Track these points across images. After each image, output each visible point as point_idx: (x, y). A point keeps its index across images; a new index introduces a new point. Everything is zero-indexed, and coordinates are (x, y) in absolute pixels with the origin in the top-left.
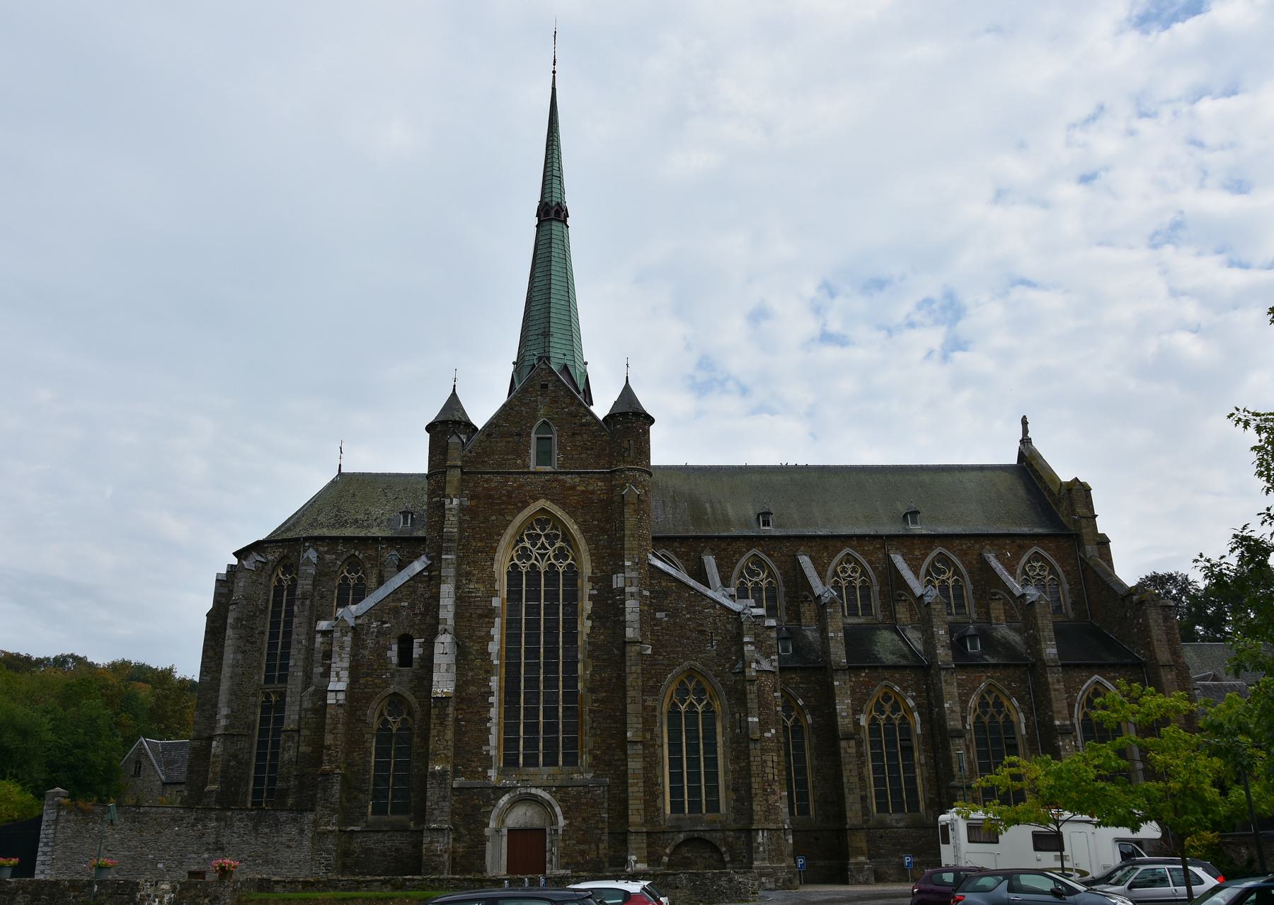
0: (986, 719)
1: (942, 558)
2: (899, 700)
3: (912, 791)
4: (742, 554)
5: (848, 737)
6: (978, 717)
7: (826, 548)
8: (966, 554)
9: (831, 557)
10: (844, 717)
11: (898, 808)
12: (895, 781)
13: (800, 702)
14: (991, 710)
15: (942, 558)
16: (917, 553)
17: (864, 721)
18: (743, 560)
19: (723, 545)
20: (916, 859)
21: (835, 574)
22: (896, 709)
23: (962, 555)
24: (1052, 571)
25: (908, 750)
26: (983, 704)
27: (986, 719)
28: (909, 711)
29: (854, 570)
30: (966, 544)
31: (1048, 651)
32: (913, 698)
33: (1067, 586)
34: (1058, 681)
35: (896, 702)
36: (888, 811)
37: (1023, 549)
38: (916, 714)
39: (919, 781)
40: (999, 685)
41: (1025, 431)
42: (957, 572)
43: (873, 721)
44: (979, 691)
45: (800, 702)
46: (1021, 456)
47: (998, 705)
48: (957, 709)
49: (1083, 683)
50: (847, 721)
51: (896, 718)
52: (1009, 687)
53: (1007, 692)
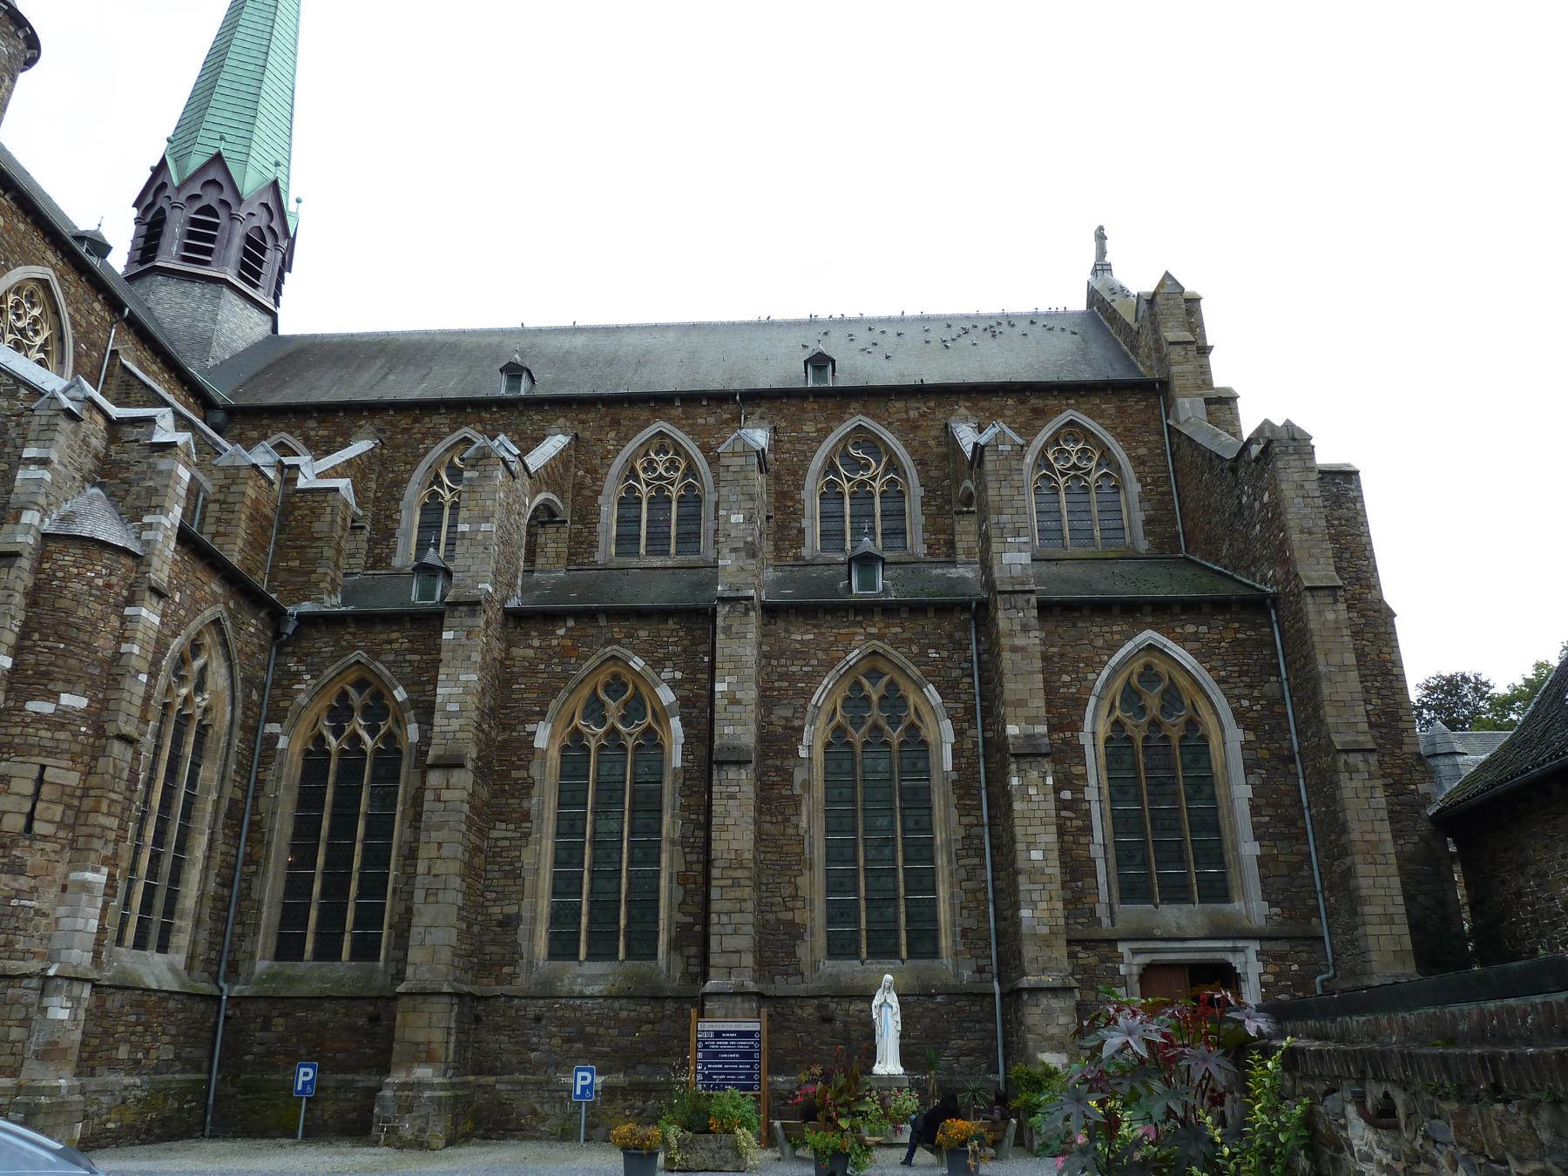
0: (858, 737)
1: (863, 438)
2: (644, 690)
3: (645, 906)
4: (438, 438)
5: (451, 764)
6: (839, 731)
7: (616, 423)
8: (915, 428)
9: (624, 439)
10: (449, 716)
11: (602, 948)
12: (605, 875)
13: (400, 694)
14: (875, 715)
15: (863, 438)
16: (809, 428)
17: (543, 736)
18: (440, 448)
19: (404, 422)
20: (620, 1079)
21: (633, 474)
22: (634, 710)
23: (908, 429)
24: (1107, 457)
25: (648, 806)
26: (856, 702)
27: (858, 737)
28: (661, 715)
29: (672, 466)
30: (915, 409)
31: (1008, 558)
32: (674, 685)
33: (1134, 488)
34: (1025, 629)
35: (637, 697)
36: (575, 956)
37: (1041, 415)
38: (675, 723)
39: (664, 882)
40: (897, 656)
41: (1101, 252)
42: (893, 465)
43: (574, 746)
44: (842, 667)
45: (400, 694)
46: (1093, 296)
47: (894, 701)
48: (750, 694)
49: (1113, 648)
50: (455, 724)
51: (630, 735)
52: (920, 659)
53: (915, 671)
